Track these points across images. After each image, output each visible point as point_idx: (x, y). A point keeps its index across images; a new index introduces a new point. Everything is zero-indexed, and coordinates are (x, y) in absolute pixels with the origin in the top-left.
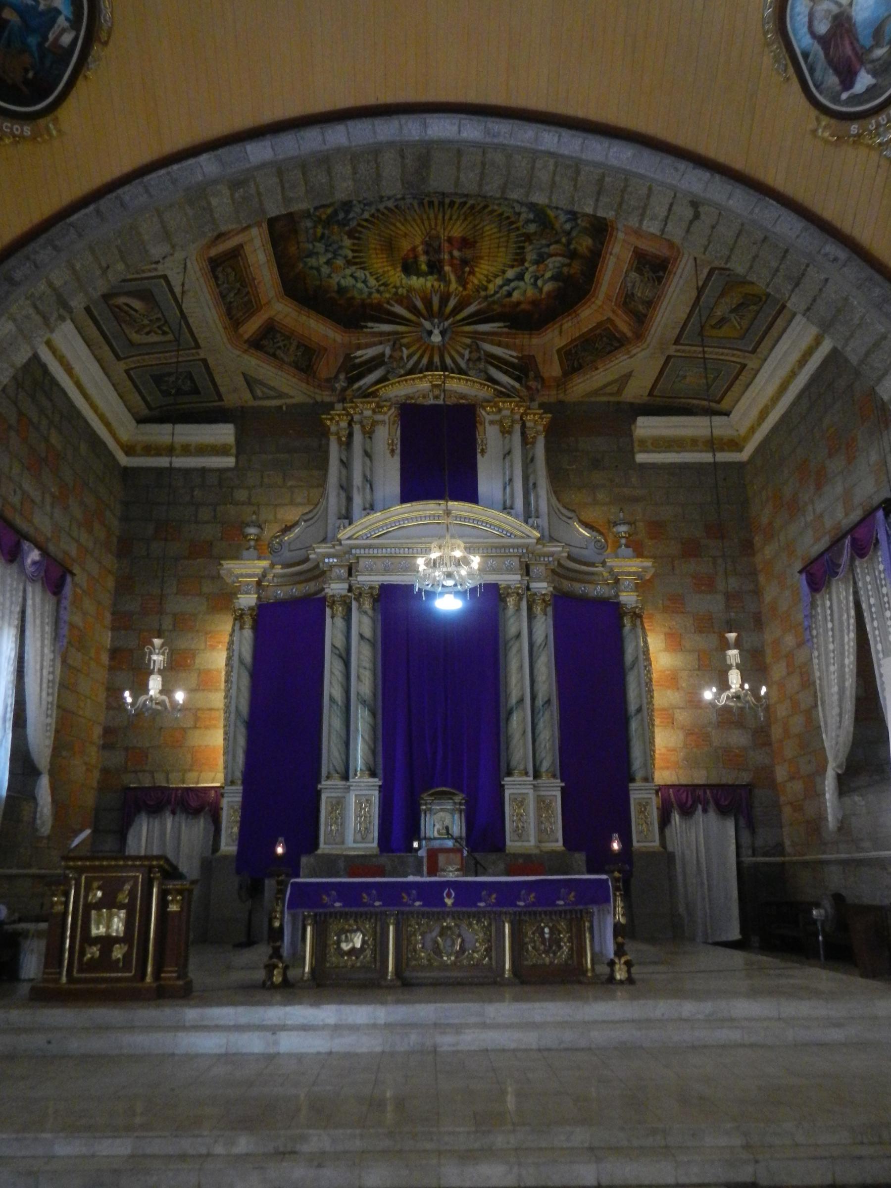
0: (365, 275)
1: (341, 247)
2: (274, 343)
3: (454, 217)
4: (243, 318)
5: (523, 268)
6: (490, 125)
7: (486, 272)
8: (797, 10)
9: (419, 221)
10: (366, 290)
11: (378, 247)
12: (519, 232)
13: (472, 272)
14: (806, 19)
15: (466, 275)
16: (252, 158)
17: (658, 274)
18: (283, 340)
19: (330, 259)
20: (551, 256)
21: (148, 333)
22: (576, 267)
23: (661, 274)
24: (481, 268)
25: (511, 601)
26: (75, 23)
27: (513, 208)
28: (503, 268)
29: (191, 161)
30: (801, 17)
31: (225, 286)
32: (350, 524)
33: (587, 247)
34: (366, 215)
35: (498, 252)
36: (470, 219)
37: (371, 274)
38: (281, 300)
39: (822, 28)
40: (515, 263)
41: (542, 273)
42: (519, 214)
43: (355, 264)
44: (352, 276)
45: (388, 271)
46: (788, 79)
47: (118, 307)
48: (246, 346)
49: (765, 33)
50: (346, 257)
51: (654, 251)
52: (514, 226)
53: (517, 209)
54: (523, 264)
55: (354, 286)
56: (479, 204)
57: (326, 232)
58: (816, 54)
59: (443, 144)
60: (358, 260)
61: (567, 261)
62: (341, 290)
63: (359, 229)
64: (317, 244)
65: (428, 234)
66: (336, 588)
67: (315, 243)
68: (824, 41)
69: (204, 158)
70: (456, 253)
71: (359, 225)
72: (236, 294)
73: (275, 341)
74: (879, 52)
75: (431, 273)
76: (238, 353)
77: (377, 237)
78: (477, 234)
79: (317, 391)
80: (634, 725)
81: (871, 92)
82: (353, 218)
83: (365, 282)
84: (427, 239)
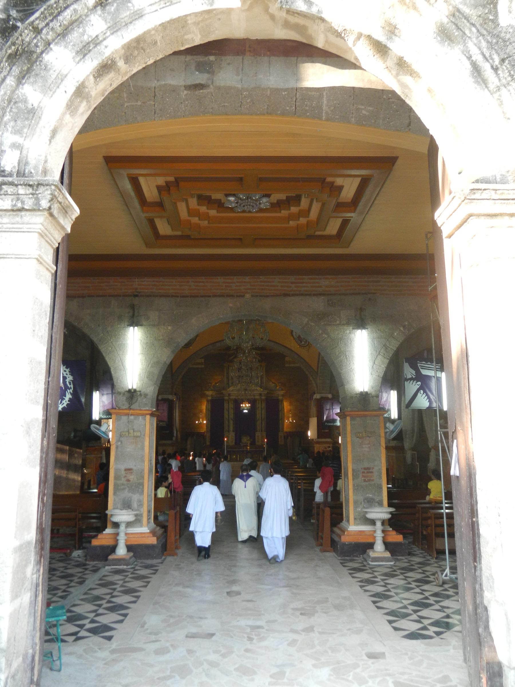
25: (258, 401)
32: (229, 388)
39: (297, 336)
66: (226, 398)
68: (298, 337)
80: (280, 422)
81: (304, 344)
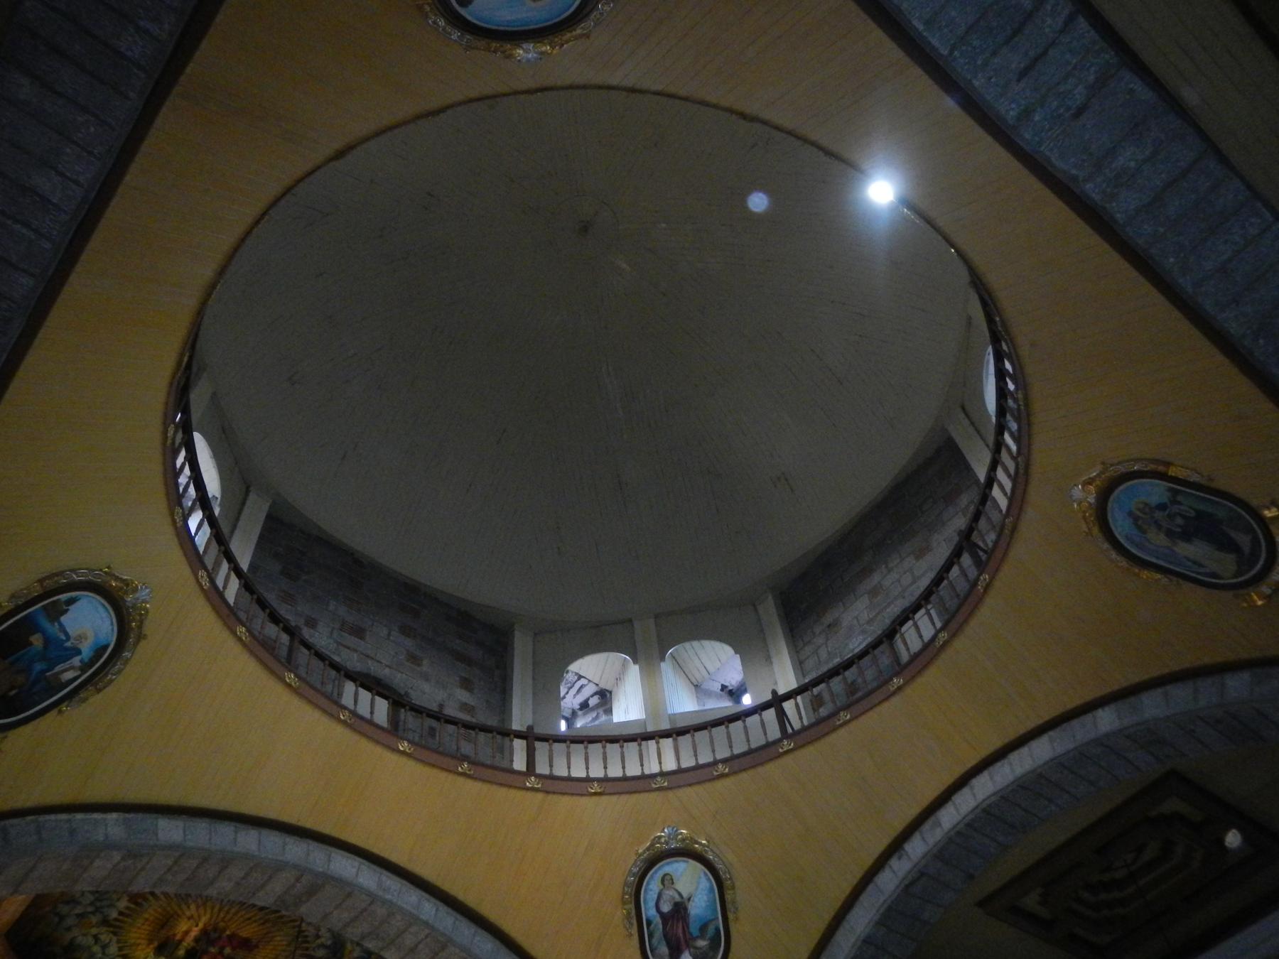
1: (111, 906)
6: (384, 878)
8: (651, 887)
9: (216, 910)
12: (308, 953)
14: (656, 896)
16: (160, 835)
26: (85, 667)
29: (96, 816)
30: (651, 893)
37: (118, 942)
39: (666, 908)
45: (139, 945)
46: (631, 935)
49: (624, 894)
55: (89, 947)
58: (656, 926)
59: (339, 882)
60: (118, 923)
69: (114, 815)
74: (702, 943)
84: (210, 928)
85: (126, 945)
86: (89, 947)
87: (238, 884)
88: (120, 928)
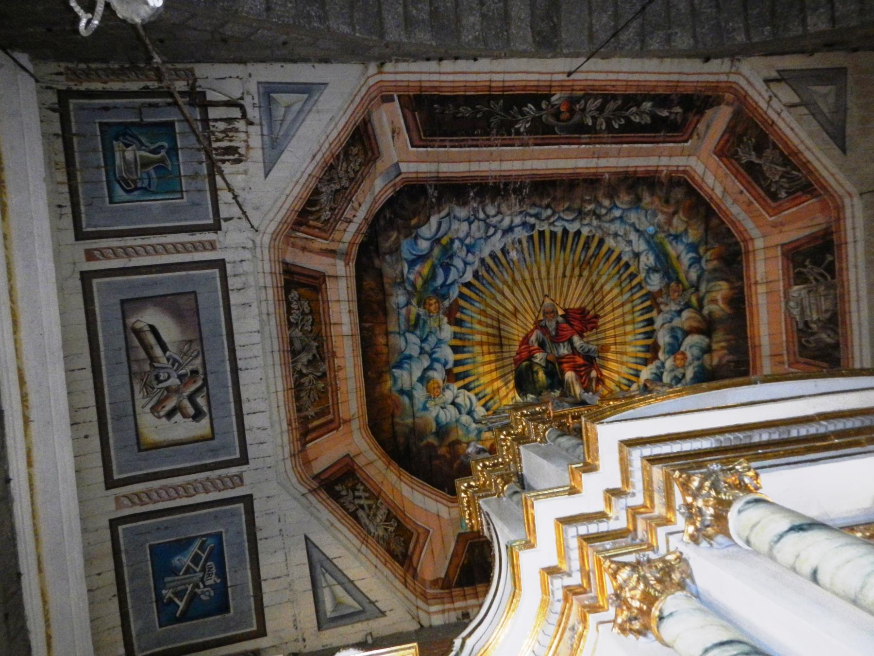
0: (470, 399)
1: (440, 341)
2: (355, 497)
3: (568, 273)
4: (316, 423)
5: (657, 363)
7: (616, 377)
9: (529, 282)
10: (474, 425)
11: (485, 338)
12: (643, 292)
13: (600, 380)
15: (594, 384)
17: (826, 262)
18: (367, 498)
19: (426, 370)
20: (686, 333)
21: (170, 415)
22: (720, 341)
23: (830, 258)
24: (610, 370)
27: (630, 242)
28: (634, 366)
31: (297, 333)
33: (723, 299)
34: (469, 277)
35: (625, 334)
36: (586, 273)
38: (363, 431)
40: (648, 355)
41: (681, 370)
42: (637, 255)
43: (458, 377)
44: (453, 403)
45: (498, 389)
47: (138, 333)
48: (315, 485)
50: (445, 364)
51: (808, 232)
52: (634, 283)
53: (636, 250)
54: (656, 357)
55: (457, 421)
56: (594, 236)
57: (422, 311)
61: (707, 340)
62: (442, 431)
63: (462, 303)
64: (409, 336)
65: (541, 306)
67: (407, 335)
70: (577, 340)
71: (462, 296)
72: (310, 363)
73: (357, 494)
75: (551, 387)
76: (304, 491)
77: (483, 319)
78: (597, 300)
79: (420, 603)
82: (452, 283)
83: (470, 413)
84: (541, 317)
85: (487, 398)
86: (457, 421)
87: (483, 16)
88: (466, 375)
